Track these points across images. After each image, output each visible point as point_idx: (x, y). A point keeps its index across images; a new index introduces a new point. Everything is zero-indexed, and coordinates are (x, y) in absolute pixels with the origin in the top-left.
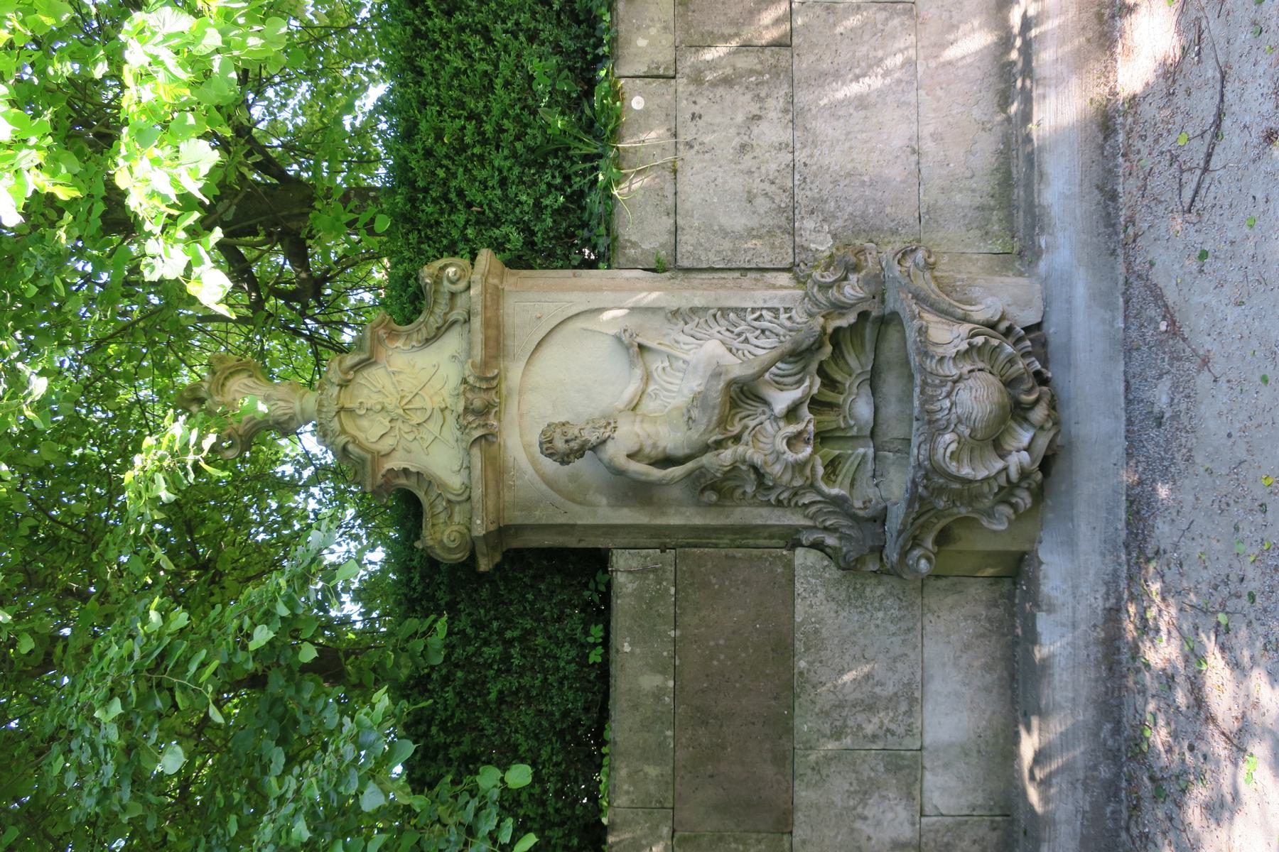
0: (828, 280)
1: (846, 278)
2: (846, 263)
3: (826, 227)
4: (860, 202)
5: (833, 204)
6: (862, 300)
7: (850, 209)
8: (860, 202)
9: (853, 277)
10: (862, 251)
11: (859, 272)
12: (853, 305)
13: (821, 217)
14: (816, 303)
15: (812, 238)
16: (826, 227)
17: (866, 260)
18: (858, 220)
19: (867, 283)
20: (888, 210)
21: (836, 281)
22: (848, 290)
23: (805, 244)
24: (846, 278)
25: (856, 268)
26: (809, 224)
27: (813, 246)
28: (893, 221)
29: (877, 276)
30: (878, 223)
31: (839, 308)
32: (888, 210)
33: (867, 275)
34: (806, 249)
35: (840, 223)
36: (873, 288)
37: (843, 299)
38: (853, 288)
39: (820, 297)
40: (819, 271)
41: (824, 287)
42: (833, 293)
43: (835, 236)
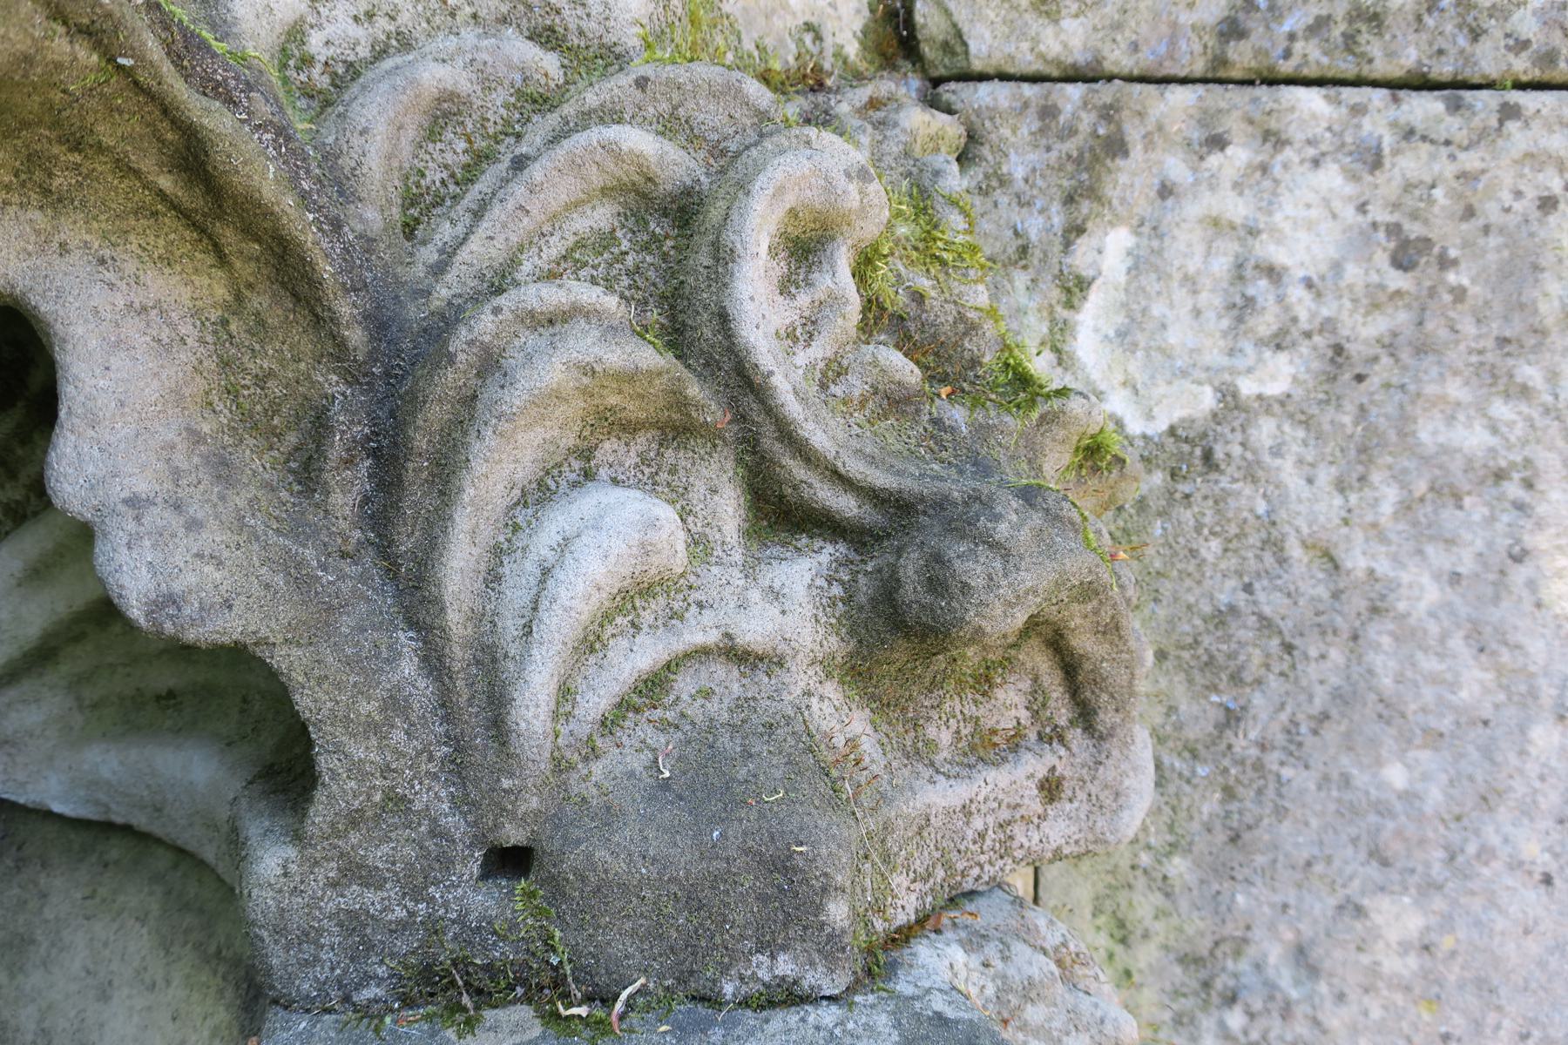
0: (759, 307)
1: (780, 515)
2: (962, 519)
3: (1276, 376)
4: (1474, 684)
5: (1473, 439)
6: (474, 703)
7: (1421, 592)
8: (1474, 684)
9: (789, 602)
10: (1083, 697)
11: (857, 674)
12: (412, 591)
13: (1364, 331)
14: (480, 145)
15: (1186, 246)
16: (1276, 376)
17: (986, 749)
18: (1325, 666)
19: (704, 780)
20: (1398, 918)
21: (743, 382)
22: (616, 529)
23: (1129, 179)
24: (780, 515)
25: (900, 632)
26: (1311, 221)
27: (1109, 250)
28: (1301, 954)
29: (789, 896)
30: (1295, 839)
31: (369, 413)
32: (1398, 918)
33: (822, 769)
34: (1083, 188)
35: (1306, 497)
36: (630, 851)
37: (495, 469)
38: (636, 597)
39: (556, 197)
40: (872, 209)
41: (673, 232)
42: (595, 344)
43: (1194, 453)
